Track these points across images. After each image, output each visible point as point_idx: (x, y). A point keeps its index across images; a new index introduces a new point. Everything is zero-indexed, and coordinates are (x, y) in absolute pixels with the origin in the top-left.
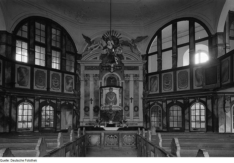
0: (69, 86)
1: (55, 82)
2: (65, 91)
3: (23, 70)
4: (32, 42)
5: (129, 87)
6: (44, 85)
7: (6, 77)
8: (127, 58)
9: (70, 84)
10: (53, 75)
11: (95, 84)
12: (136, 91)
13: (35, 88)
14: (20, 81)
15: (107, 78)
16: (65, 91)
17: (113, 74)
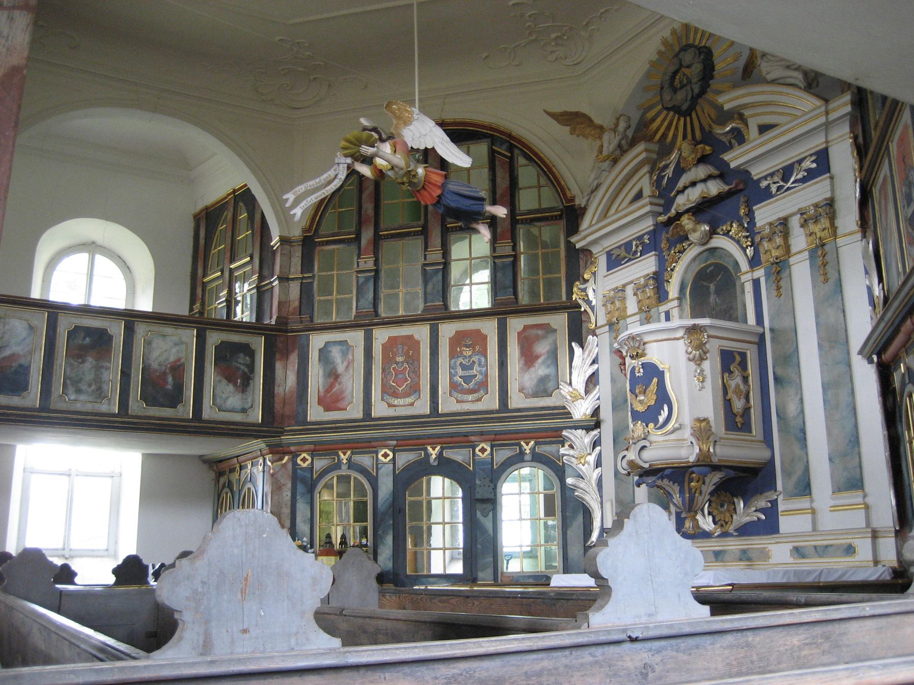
1: (464, 367)
2: (516, 400)
3: (336, 353)
6: (415, 389)
7: (279, 390)
8: (764, 129)
9: (540, 360)
10: (458, 340)
12: (831, 315)
14: (325, 396)
16: (516, 400)
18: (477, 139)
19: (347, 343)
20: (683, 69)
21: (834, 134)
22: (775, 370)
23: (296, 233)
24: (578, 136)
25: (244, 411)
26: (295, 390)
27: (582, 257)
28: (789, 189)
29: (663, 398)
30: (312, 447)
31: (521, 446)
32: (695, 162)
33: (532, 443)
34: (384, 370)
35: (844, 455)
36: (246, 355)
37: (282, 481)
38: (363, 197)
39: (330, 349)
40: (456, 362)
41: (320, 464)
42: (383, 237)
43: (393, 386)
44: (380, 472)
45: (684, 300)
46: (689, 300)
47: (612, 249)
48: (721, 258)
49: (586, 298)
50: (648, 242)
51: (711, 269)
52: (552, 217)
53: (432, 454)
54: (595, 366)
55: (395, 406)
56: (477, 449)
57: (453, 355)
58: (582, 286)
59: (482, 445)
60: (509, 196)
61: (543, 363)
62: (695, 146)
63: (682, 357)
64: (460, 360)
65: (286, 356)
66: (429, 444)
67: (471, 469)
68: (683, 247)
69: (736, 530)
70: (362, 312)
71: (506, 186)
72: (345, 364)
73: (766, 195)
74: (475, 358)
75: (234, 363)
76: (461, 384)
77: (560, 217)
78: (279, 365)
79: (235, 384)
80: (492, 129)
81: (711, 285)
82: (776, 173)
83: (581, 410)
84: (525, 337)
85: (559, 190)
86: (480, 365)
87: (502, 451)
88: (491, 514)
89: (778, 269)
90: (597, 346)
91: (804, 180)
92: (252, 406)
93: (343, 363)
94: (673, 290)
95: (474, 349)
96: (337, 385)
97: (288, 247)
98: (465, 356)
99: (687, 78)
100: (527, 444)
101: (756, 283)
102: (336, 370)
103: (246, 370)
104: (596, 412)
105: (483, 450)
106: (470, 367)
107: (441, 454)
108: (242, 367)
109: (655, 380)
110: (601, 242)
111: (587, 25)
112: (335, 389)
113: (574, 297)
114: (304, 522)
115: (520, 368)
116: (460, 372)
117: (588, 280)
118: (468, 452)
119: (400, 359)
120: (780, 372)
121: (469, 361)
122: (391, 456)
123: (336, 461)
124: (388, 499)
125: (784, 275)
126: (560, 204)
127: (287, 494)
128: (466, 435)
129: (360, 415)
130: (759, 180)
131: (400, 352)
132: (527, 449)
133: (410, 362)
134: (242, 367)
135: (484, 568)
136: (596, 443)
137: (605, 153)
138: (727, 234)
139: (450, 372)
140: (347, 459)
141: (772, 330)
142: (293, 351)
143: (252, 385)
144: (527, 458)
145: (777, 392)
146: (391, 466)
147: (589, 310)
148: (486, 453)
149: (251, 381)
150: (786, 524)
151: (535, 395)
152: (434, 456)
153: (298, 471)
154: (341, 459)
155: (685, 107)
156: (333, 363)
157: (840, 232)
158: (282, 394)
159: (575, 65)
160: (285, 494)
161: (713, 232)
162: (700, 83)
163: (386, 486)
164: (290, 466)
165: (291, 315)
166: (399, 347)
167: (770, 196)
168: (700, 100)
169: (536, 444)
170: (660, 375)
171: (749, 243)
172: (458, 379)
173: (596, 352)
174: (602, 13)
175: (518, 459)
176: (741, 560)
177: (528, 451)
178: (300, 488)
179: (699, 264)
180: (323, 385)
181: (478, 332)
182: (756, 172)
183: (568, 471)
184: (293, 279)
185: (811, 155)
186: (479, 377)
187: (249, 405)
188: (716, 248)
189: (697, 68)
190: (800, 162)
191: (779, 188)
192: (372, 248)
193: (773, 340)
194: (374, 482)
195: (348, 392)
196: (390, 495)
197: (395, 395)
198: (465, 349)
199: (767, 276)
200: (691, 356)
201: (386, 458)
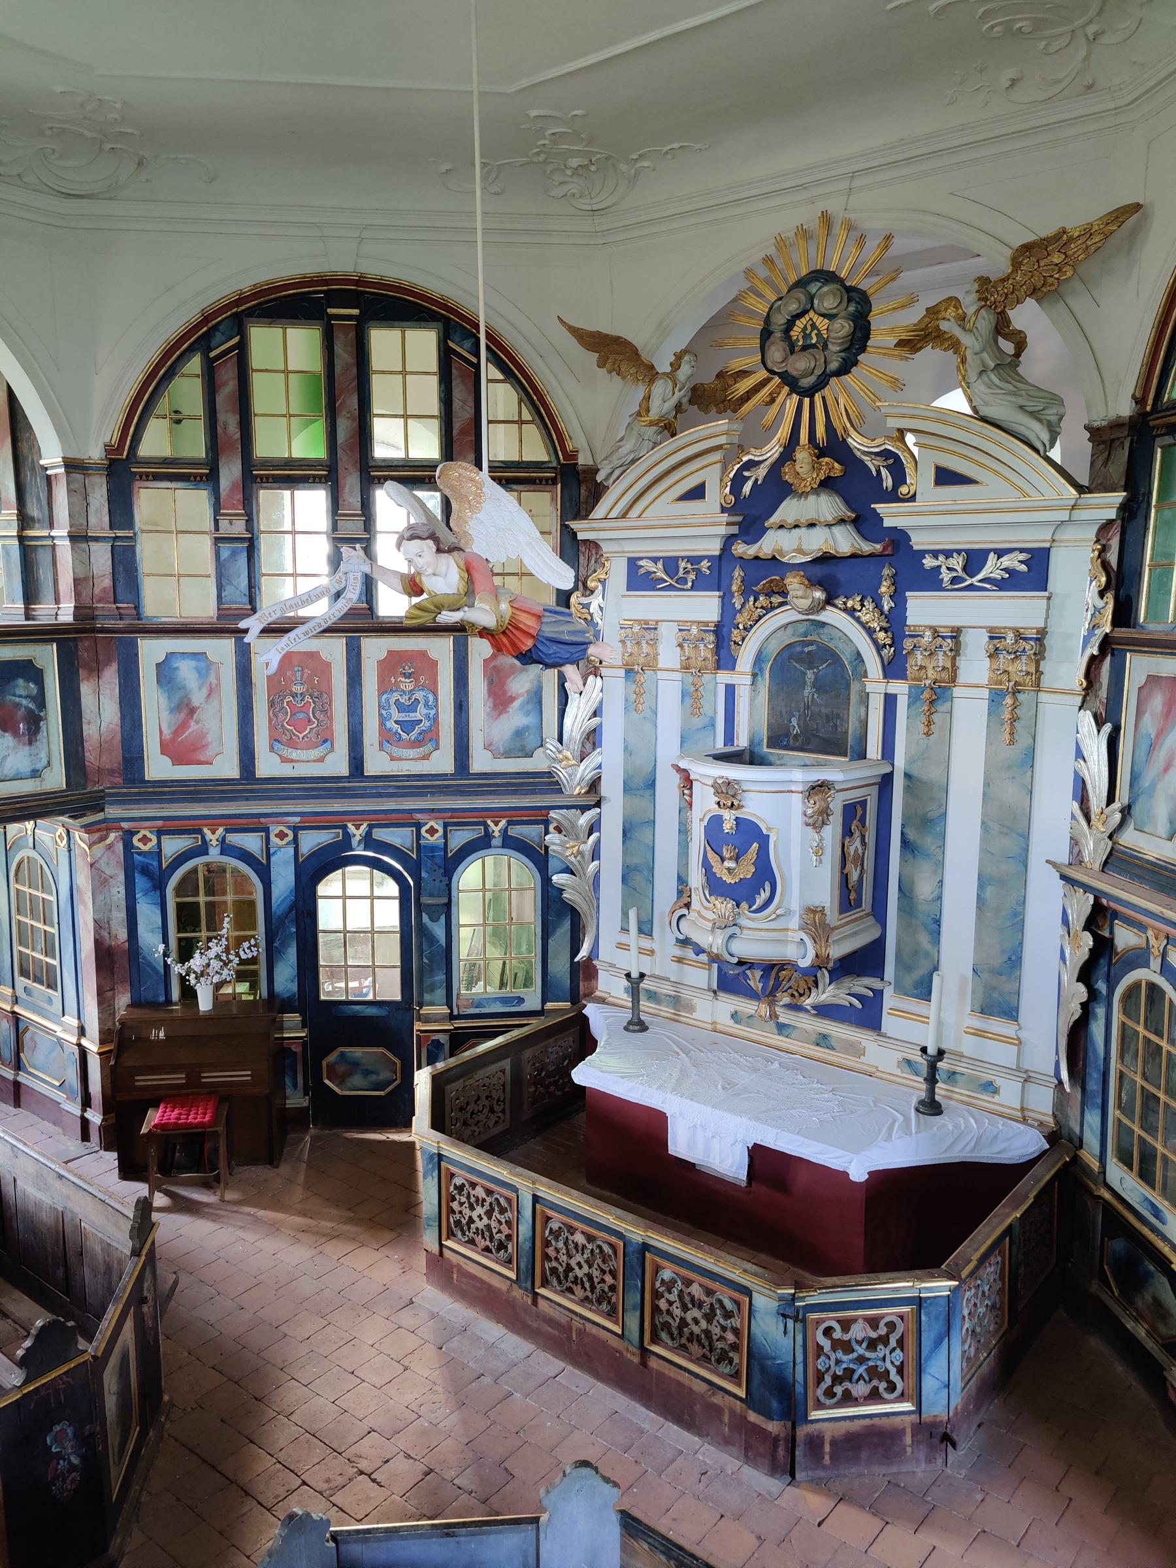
0: (516, 718)
1: (401, 708)
2: (481, 762)
3: (186, 671)
4: (230, 473)
6: (326, 739)
7: (90, 731)
8: (945, 477)
9: (516, 704)
10: (392, 664)
11: (689, 701)
12: (1010, 792)
13: (267, 765)
14: (173, 740)
15: (774, 648)
16: (481, 762)
18: (417, 320)
19: (207, 658)
20: (812, 314)
21: (1067, 534)
22: (906, 830)
23: (95, 453)
25: (35, 774)
26: (119, 728)
27: (583, 549)
28: (971, 588)
29: (764, 874)
30: (160, 823)
31: (486, 826)
33: (503, 823)
34: (272, 704)
35: (998, 972)
36: (28, 680)
37: (109, 871)
38: (220, 399)
39: (176, 665)
40: (388, 700)
41: (173, 846)
42: (259, 480)
43: (287, 730)
44: (273, 859)
45: (760, 679)
46: (768, 680)
47: (642, 559)
49: (589, 618)
51: (810, 648)
52: (541, 479)
53: (355, 835)
54: (597, 720)
55: (292, 761)
56: (423, 830)
57: (384, 688)
58: (585, 600)
59: (431, 823)
60: (473, 434)
61: (521, 707)
62: (818, 457)
63: (797, 820)
64: (396, 696)
65: (96, 670)
66: (349, 821)
67: (414, 856)
68: (771, 603)
69: (814, 1008)
70: (230, 609)
71: (469, 416)
72: (205, 691)
73: (931, 581)
74: (419, 695)
75: (9, 698)
76: (396, 732)
77: (554, 481)
78: (86, 690)
79: (15, 733)
80: (445, 306)
82: (955, 555)
83: (574, 778)
84: (495, 667)
85: (555, 437)
86: (426, 705)
87: (461, 832)
88: (443, 918)
89: (934, 697)
90: (602, 691)
91: (1001, 585)
92: (49, 762)
93: (200, 689)
94: (746, 657)
95: (417, 680)
96: (193, 723)
97: (79, 477)
98: (404, 691)
99: (819, 335)
100: (496, 824)
101: (890, 701)
102: (189, 701)
103: (32, 706)
104: (594, 785)
105: (432, 831)
106: (412, 707)
107: (368, 834)
108: (24, 702)
109: (755, 846)
112: (190, 730)
114: (152, 931)
115: (488, 714)
116: (396, 715)
117: (592, 592)
118: (410, 833)
119: (299, 689)
120: (911, 835)
121: (409, 699)
122: (291, 837)
123: (200, 843)
124: (286, 898)
125: (943, 707)
127: (118, 891)
128: (411, 811)
129: (233, 772)
130: (923, 553)
131: (299, 678)
132: (496, 830)
133: (316, 694)
134: (24, 702)
135: (432, 989)
136: (593, 828)
137: (654, 414)
138: (851, 612)
139: (380, 715)
140: (217, 840)
141: (907, 776)
142: (108, 663)
143: (44, 728)
144: (496, 842)
145: (903, 860)
146: (291, 850)
148: (437, 835)
149: (42, 723)
150: (889, 1023)
151: (507, 754)
152: (358, 838)
153: (136, 856)
154: (208, 839)
155: (806, 382)
156: (184, 687)
157: (1046, 681)
158: (96, 736)
160: (114, 891)
161: (829, 601)
162: (843, 354)
163: (284, 880)
164: (120, 847)
165: (99, 601)
166: (296, 669)
168: (834, 381)
169: (509, 823)
170: (764, 840)
171: (888, 641)
172: (390, 724)
175: (482, 844)
176: (818, 1045)
177: (497, 834)
178: (141, 882)
180: (169, 723)
181: (423, 654)
182: (918, 541)
183: (553, 864)
184: (96, 539)
185: (1022, 550)
186: (426, 724)
187: (44, 762)
188: (823, 624)
189: (843, 328)
190: (1000, 553)
191: (954, 580)
192: (240, 496)
193: (907, 789)
194: (264, 872)
195: (210, 738)
196: (291, 892)
197: (292, 744)
198: (403, 680)
199: (914, 698)
200: (811, 821)
201: (282, 840)
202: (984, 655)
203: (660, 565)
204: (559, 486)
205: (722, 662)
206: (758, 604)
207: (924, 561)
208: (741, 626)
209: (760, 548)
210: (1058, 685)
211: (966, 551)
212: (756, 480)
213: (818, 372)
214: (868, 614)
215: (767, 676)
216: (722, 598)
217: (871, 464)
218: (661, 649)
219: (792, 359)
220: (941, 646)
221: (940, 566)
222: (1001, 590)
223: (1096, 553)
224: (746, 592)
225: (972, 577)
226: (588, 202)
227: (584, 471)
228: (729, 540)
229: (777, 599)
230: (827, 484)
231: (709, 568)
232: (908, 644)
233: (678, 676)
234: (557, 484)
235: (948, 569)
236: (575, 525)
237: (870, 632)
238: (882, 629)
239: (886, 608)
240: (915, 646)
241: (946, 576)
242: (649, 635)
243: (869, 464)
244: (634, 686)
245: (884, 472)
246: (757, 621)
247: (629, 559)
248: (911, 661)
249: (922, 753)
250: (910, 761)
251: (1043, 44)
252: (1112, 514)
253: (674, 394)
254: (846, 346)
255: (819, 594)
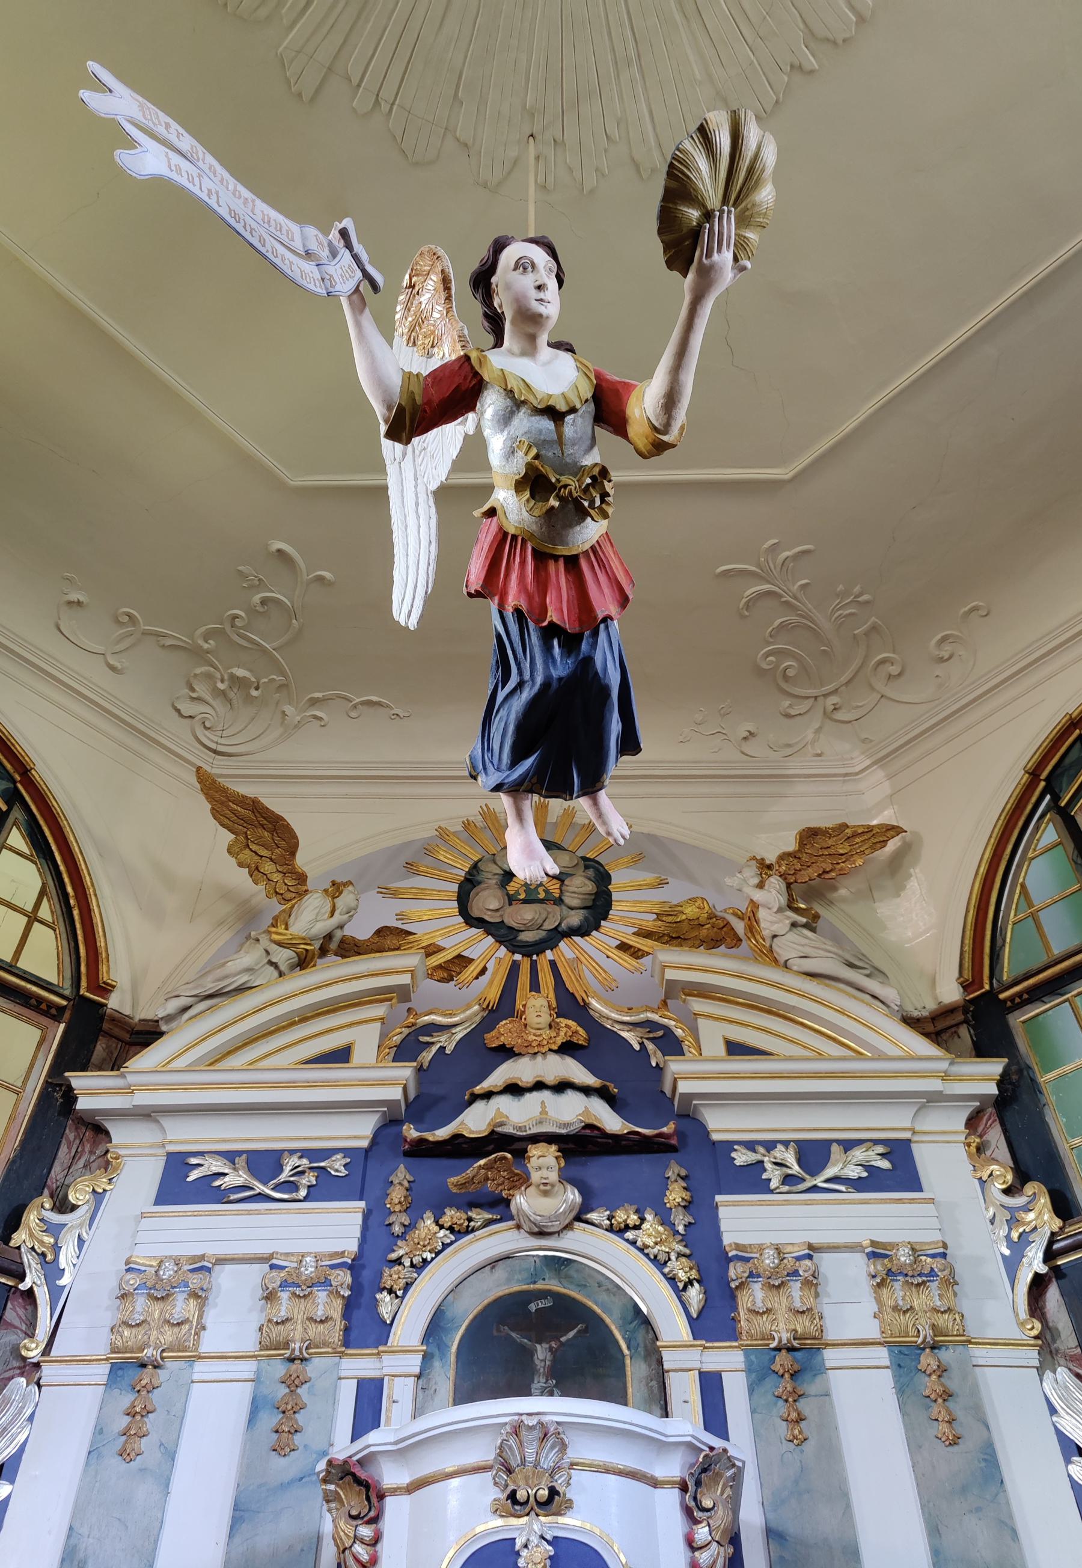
5: (832, 1452)
11: (269, 1420)
17: (558, 1265)
24: (241, 865)
27: (71, 1136)
28: (814, 1189)
32: (555, 1047)
45: (437, 1364)
46: (453, 1366)
48: (582, 1287)
50: (343, 1172)
58: (56, 1218)
68: (470, 1220)
77: (53, 1013)
81: (538, 1347)
82: (780, 1147)
89: (796, 1367)
91: (858, 1184)
110: (167, 1122)
111: (314, 702)
113: (19, 1237)
117: (74, 1208)
125: (811, 1388)
126: (67, 984)
130: (730, 1145)
138: (620, 1231)
141: (772, 1534)
147: (42, 1295)
155: (527, 937)
159: (215, 752)
167: (764, 1187)
171: (694, 1274)
173: (22, 1438)
174: (370, 703)
179: (509, 1280)
185: (876, 1142)
190: (848, 1145)
191: (788, 1179)
202: (865, 1287)
203: (241, 1161)
204: (62, 1026)
205: (354, 1334)
206: (446, 1220)
207: (733, 1155)
208: (407, 1263)
209: (462, 1123)
210: (991, 1334)
211: (796, 1142)
212: (442, 1048)
213: (549, 925)
214: (651, 1230)
215: (453, 1358)
216: (367, 1216)
217: (632, 1037)
218: (209, 1319)
219: (509, 910)
220: (796, 1273)
221: (762, 1162)
222: (859, 1191)
223: (973, 1149)
224: (414, 1208)
225: (813, 1174)
226: (215, 739)
227: (113, 1020)
228: (391, 1122)
229: (479, 1216)
230: (568, 1049)
231: (345, 1166)
232: (735, 1271)
233: (247, 1368)
234: (57, 1019)
235: (776, 1164)
236: (78, 1081)
237: (659, 1263)
238: (680, 1255)
239: (681, 1229)
240: (751, 1275)
241: (774, 1176)
242: (195, 1281)
243: (624, 1034)
244: (126, 1400)
245: (650, 1046)
246: (438, 1254)
247: (170, 1155)
248: (744, 1301)
249: (796, 1482)
250: (771, 1503)
251: (787, 703)
252: (992, 1089)
253: (332, 914)
254: (590, 904)
255: (573, 1196)
